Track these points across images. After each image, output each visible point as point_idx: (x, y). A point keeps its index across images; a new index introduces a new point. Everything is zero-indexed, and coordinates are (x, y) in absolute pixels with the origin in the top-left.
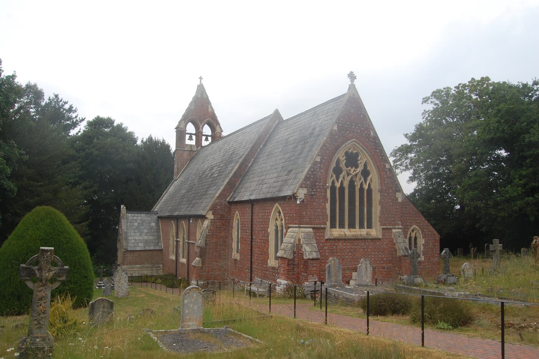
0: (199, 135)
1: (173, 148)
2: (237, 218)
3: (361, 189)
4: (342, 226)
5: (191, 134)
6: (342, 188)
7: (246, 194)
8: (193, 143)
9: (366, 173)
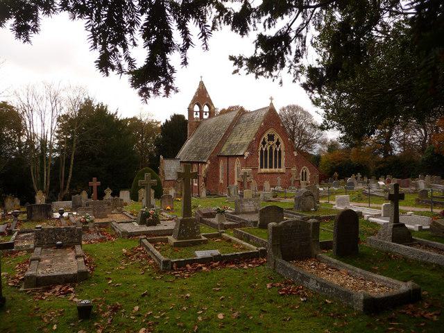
0: (201, 112)
1: (187, 118)
2: (222, 164)
3: (276, 151)
4: (266, 167)
5: (197, 112)
6: (266, 151)
7: (225, 150)
8: (198, 116)
9: (278, 143)
